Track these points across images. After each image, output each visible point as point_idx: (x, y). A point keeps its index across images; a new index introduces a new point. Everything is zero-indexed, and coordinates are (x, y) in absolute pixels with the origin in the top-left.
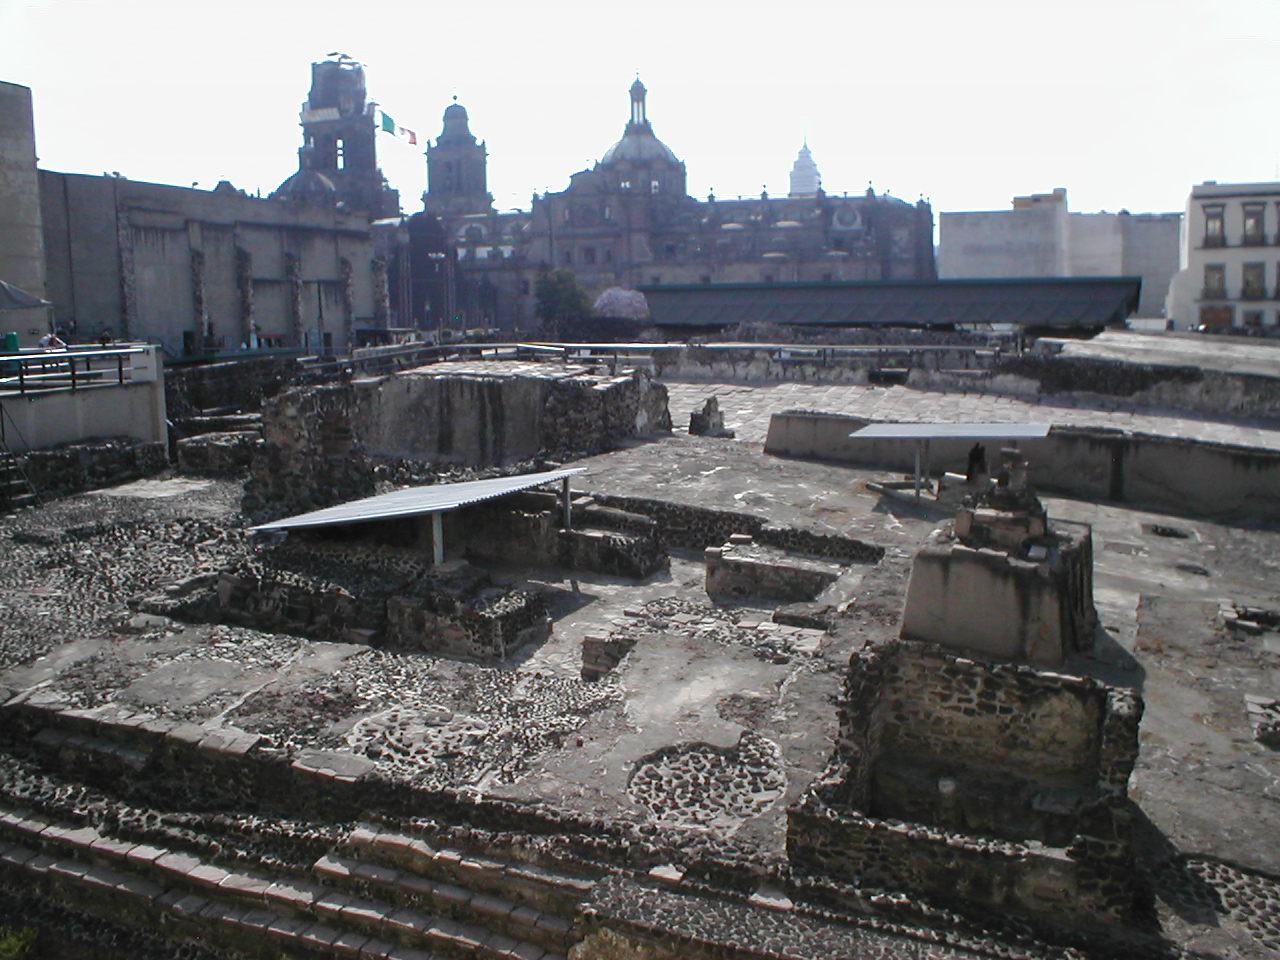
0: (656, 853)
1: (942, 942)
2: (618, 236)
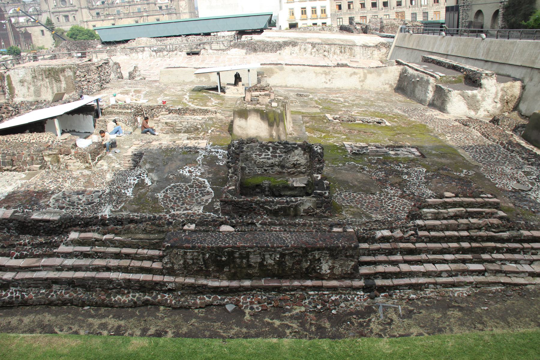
0: (183, 221)
1: (285, 231)
2: (77, 11)
